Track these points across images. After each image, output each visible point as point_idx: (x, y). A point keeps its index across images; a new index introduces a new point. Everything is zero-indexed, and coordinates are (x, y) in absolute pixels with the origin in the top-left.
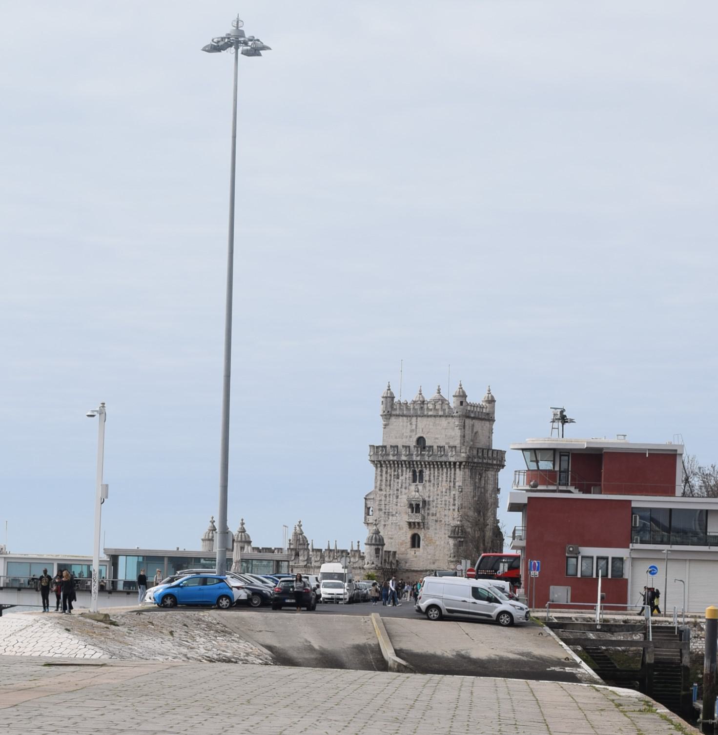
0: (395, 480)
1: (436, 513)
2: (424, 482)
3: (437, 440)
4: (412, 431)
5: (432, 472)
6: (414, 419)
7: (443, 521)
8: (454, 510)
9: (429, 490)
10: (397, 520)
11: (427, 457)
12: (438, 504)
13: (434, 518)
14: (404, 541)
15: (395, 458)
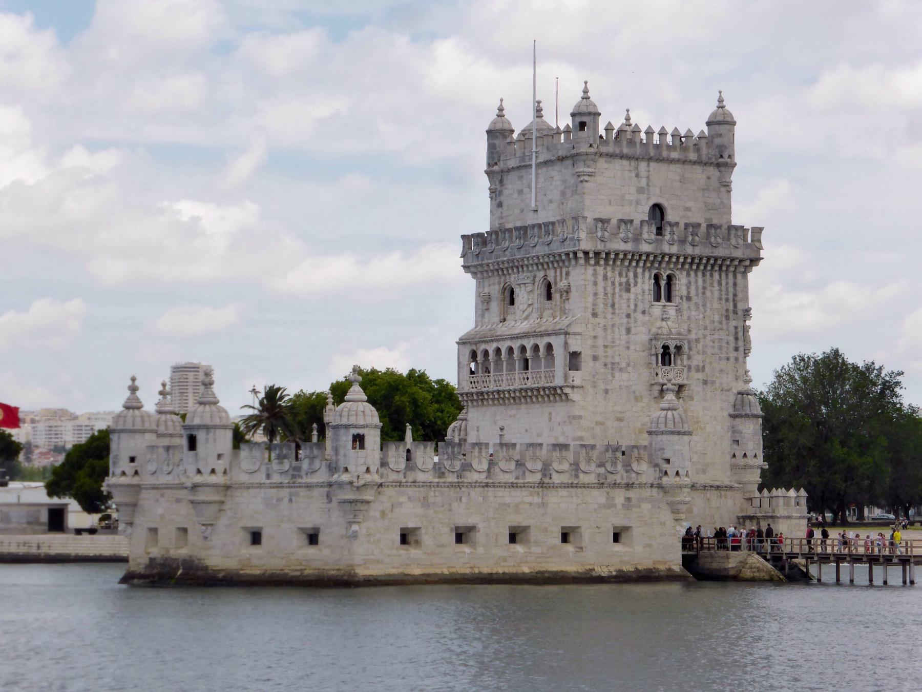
0: (625, 295)
1: (704, 366)
2: (676, 300)
3: (689, 214)
4: (640, 190)
5: (692, 278)
6: (643, 165)
7: (717, 384)
8: (737, 359)
9: (689, 318)
10: (630, 380)
11: (691, 247)
12: (706, 346)
13: (700, 376)
14: (643, 425)
15: (629, 247)
